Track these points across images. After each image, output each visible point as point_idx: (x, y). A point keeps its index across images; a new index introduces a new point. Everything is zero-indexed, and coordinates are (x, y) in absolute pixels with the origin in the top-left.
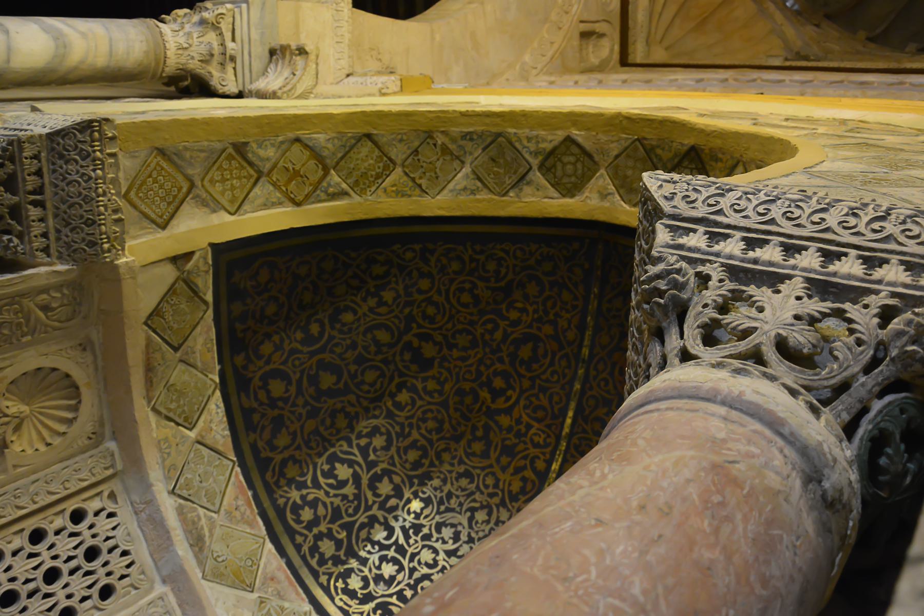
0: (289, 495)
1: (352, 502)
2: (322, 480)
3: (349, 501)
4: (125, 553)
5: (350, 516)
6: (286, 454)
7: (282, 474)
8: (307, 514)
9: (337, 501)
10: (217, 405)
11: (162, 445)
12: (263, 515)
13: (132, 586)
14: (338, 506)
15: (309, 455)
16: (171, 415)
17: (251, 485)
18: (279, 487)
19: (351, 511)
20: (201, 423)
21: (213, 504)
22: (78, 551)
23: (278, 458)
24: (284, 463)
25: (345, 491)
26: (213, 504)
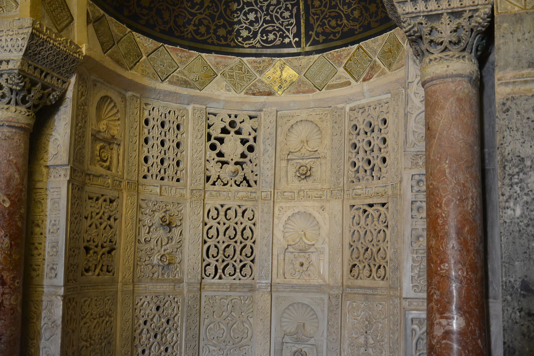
0: (189, 31)
1: (213, 6)
2: (193, 11)
3: (211, 7)
4: (169, 112)
5: (217, 12)
6: (173, 18)
7: (179, 27)
8: (203, 29)
9: (207, 12)
10: (139, 37)
11: (144, 73)
12: (191, 48)
13: (182, 117)
14: (210, 13)
15: (180, 8)
16: (135, 62)
17: (175, 44)
18: (183, 32)
19: (215, 10)
20: (142, 50)
21: (175, 67)
22: (160, 130)
23: (172, 23)
24: (175, 22)
25: (206, 5)
26: (175, 67)
